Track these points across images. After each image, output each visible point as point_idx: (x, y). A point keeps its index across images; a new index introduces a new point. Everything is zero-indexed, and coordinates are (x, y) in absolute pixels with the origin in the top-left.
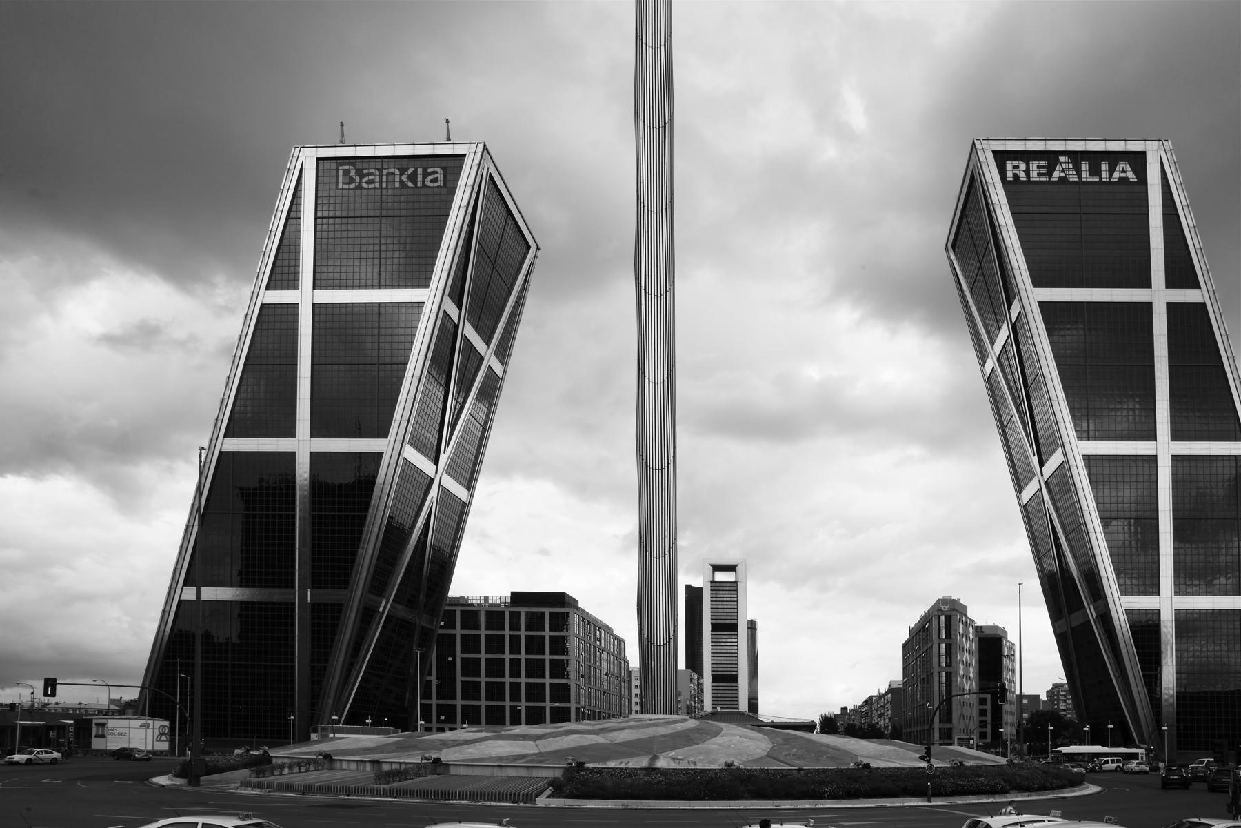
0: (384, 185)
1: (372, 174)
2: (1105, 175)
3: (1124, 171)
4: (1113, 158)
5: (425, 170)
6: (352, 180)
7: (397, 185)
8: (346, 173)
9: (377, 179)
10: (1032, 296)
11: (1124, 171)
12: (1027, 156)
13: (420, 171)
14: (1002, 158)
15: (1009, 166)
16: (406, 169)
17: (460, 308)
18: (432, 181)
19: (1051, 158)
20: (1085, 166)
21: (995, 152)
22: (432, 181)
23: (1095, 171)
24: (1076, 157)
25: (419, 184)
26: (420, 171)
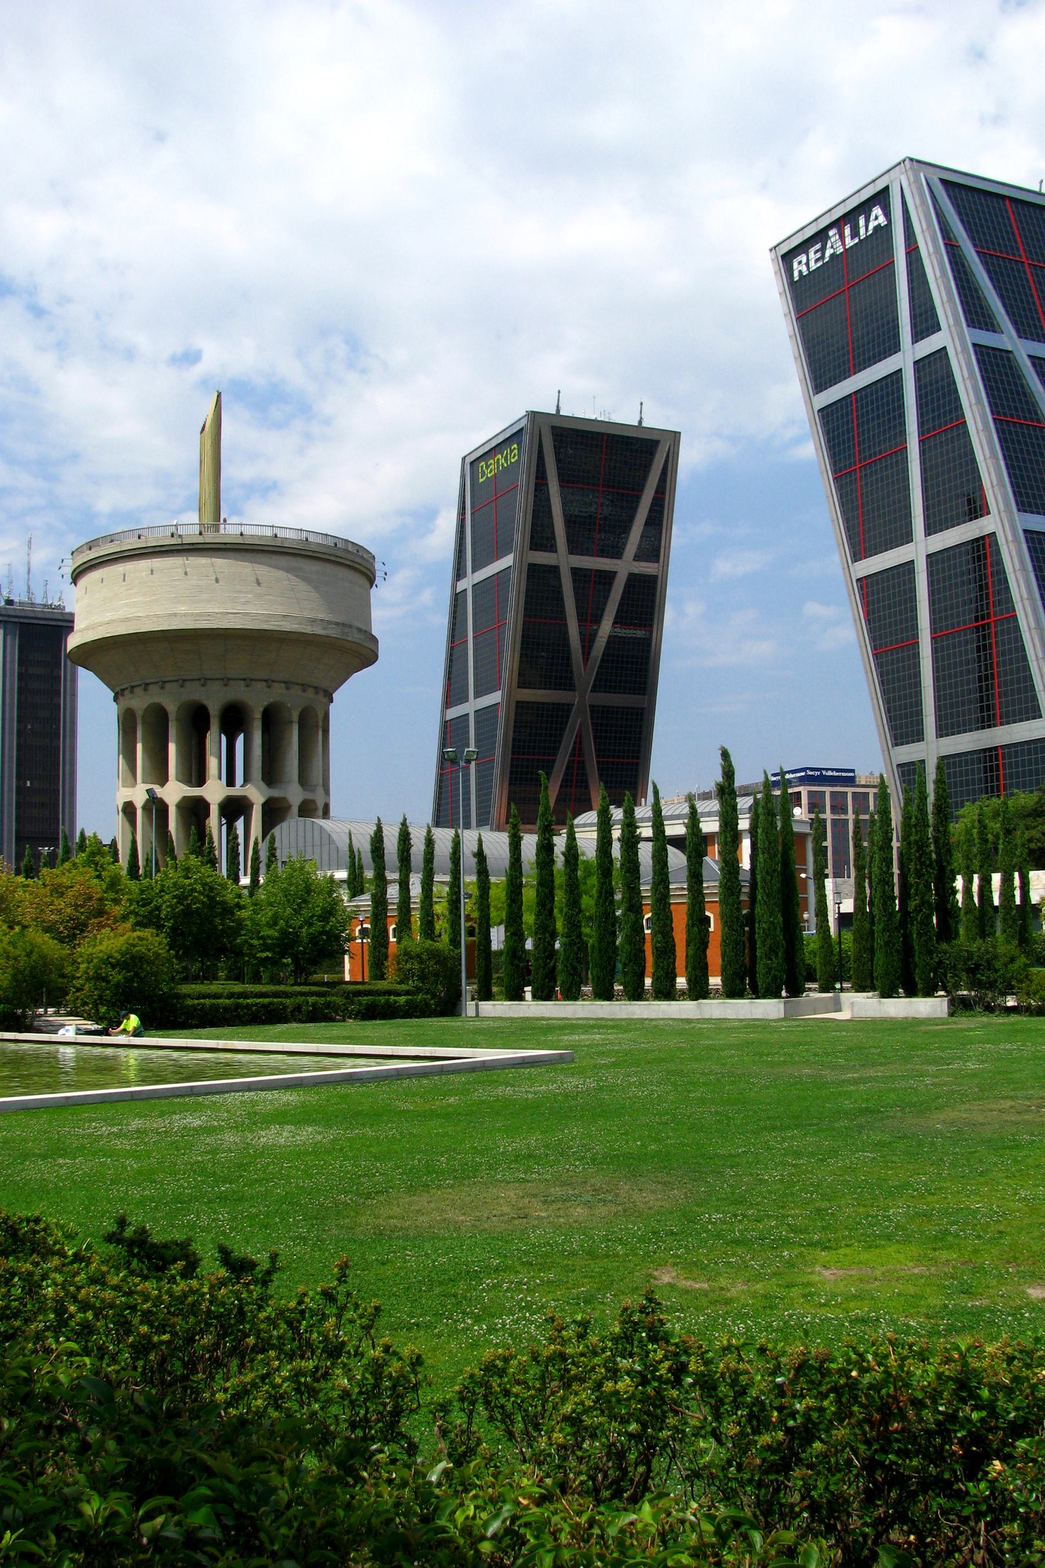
2: (862, 231)
11: (876, 218)
12: (803, 247)
15: (795, 265)
19: (821, 236)
20: (847, 231)
23: (855, 233)
24: (838, 224)
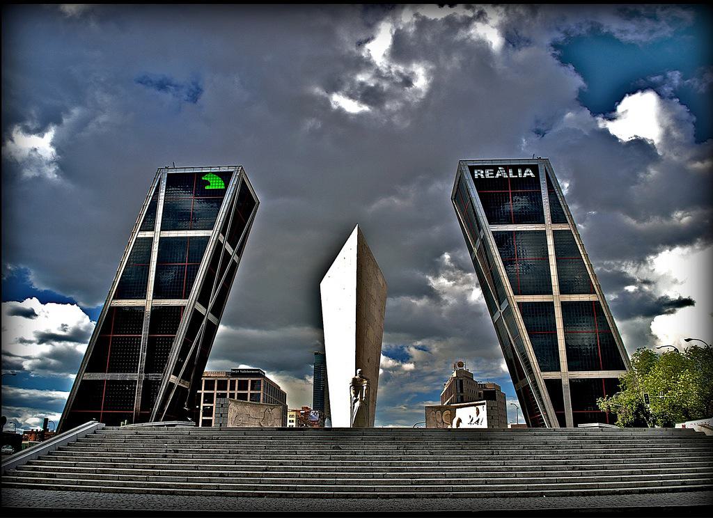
3: (529, 173)
4: (524, 168)
10: (490, 229)
12: (484, 168)
14: (472, 169)
15: (476, 172)
17: (224, 236)
19: (495, 168)
20: (510, 171)
21: (470, 167)
23: (515, 173)
24: (506, 168)
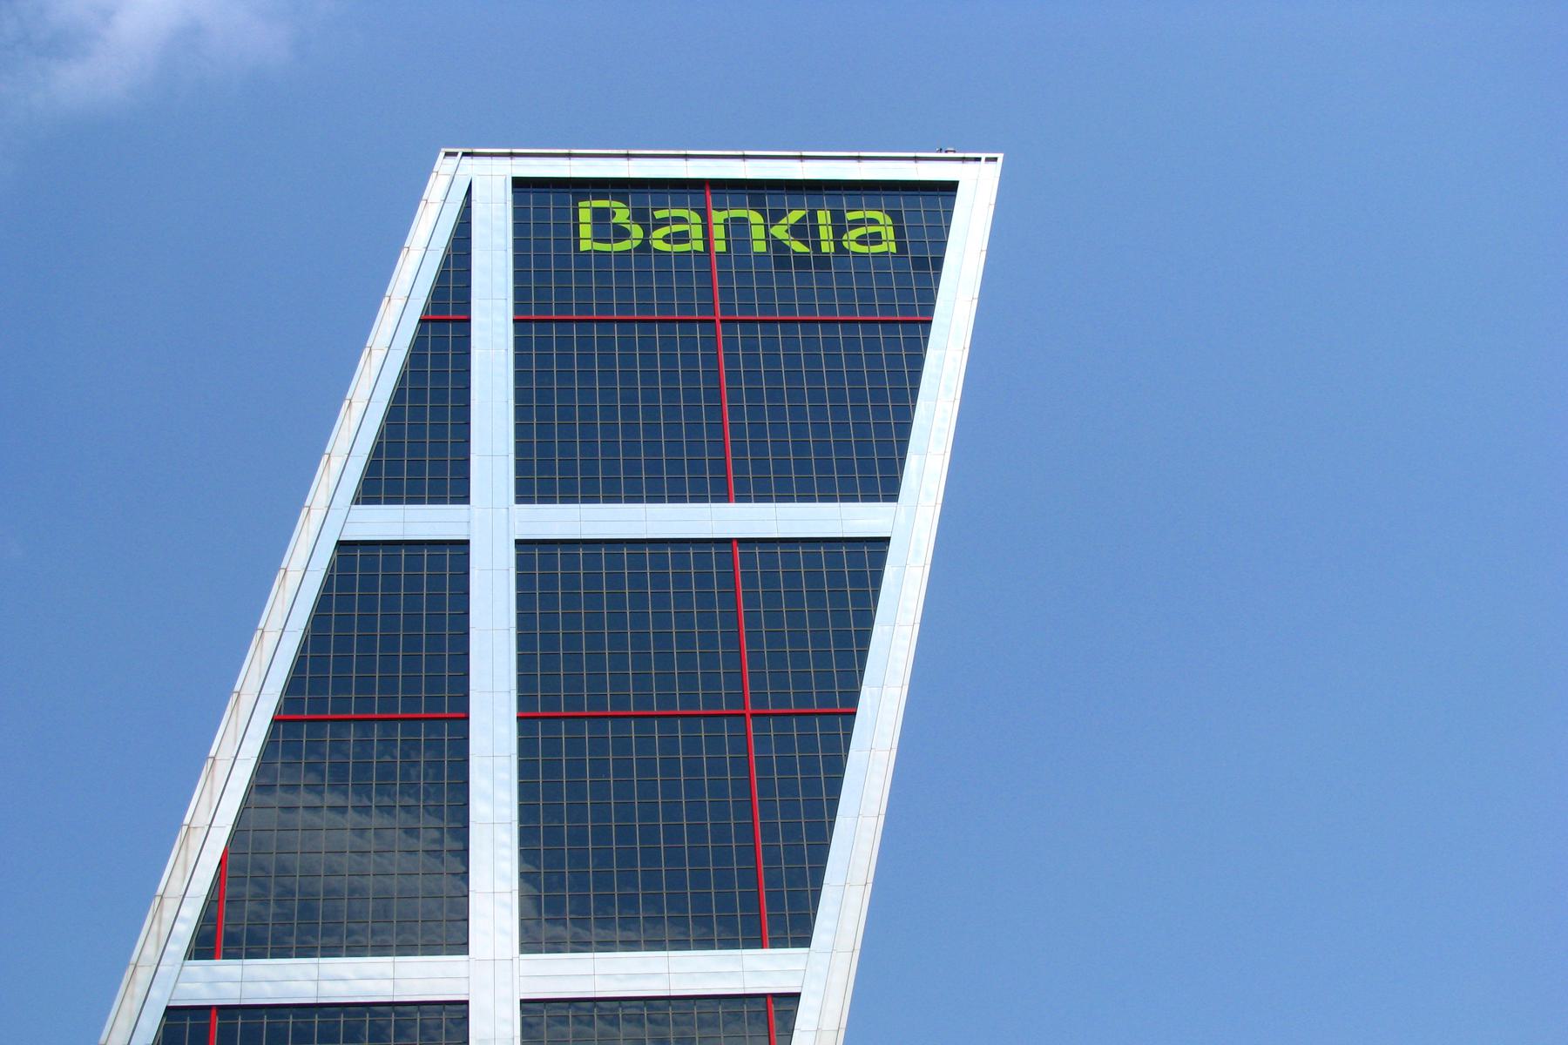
0: (720, 246)
1: (681, 220)
5: (838, 217)
6: (622, 234)
7: (760, 247)
8: (601, 216)
9: (697, 232)
13: (823, 217)
16: (783, 214)
18: (861, 240)
22: (861, 240)
25: (827, 247)
26: (823, 217)
